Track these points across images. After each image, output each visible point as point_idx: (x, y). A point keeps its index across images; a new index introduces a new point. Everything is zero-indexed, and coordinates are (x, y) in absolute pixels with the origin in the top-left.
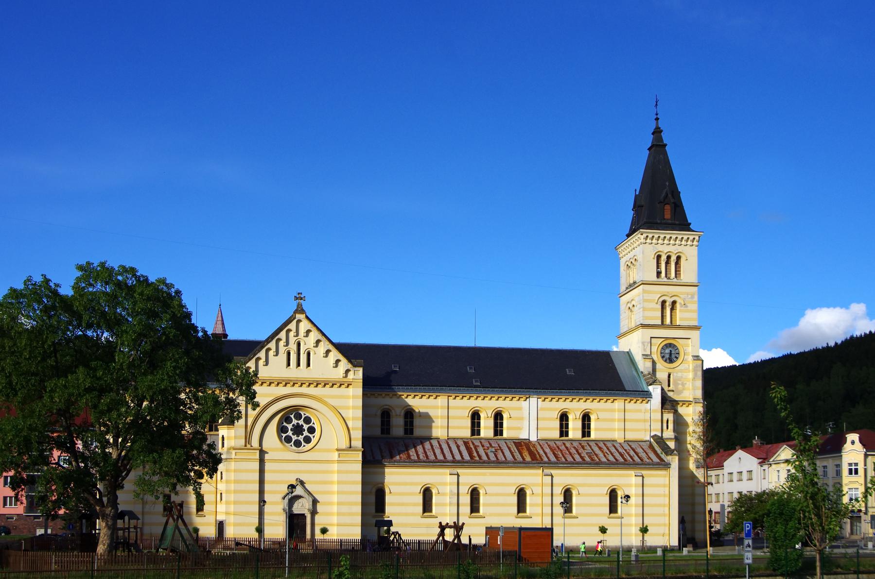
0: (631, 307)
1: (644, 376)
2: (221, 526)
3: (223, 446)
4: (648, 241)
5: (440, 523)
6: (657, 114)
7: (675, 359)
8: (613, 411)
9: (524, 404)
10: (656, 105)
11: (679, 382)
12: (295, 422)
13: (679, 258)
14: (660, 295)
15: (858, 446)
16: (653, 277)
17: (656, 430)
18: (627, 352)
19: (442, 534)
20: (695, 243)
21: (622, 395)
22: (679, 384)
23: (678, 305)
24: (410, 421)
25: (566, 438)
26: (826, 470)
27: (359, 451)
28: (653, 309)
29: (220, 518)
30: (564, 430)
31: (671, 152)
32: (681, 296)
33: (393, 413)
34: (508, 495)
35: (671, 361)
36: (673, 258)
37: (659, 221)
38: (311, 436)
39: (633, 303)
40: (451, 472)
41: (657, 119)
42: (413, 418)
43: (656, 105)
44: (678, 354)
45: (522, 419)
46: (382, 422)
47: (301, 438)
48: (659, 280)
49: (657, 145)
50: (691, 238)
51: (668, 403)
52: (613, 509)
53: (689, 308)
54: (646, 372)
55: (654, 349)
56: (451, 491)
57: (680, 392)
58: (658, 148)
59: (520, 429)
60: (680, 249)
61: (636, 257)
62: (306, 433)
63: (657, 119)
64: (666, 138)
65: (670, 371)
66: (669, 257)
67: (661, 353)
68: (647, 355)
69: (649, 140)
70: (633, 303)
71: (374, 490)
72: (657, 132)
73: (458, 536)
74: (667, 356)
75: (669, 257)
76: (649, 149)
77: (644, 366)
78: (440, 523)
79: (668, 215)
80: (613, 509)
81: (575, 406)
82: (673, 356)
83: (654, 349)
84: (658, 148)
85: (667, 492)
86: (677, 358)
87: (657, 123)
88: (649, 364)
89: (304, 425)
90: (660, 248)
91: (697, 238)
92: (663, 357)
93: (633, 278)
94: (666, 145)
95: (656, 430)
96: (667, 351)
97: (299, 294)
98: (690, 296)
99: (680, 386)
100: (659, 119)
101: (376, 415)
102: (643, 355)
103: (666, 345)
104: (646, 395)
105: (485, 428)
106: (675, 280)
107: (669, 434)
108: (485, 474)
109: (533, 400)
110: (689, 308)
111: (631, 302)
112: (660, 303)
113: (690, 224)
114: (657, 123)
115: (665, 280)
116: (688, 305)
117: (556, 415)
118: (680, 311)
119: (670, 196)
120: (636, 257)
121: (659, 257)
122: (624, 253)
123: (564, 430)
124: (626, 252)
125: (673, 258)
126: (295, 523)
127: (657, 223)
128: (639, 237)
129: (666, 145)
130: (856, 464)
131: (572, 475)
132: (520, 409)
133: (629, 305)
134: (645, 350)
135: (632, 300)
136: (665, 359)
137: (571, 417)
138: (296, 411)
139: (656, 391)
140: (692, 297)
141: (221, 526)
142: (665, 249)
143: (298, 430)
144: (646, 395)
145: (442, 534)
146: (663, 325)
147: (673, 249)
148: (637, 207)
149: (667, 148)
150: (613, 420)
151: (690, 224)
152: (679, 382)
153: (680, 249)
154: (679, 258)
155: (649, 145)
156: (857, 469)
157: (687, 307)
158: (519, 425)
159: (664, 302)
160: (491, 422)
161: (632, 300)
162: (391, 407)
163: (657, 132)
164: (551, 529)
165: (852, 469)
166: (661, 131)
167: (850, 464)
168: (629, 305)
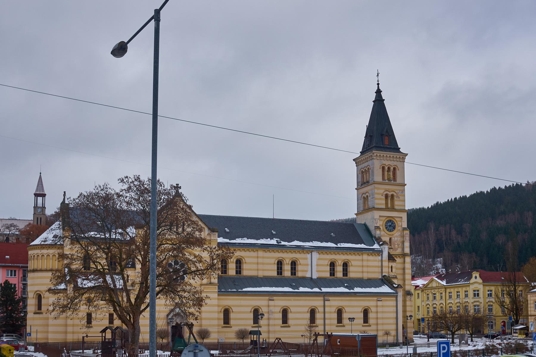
0: (365, 196)
6: (378, 81)
10: (378, 75)
11: (396, 243)
13: (394, 169)
15: (479, 280)
17: (385, 273)
18: (364, 224)
22: (395, 245)
24: (333, 268)
26: (451, 294)
27: (216, 285)
28: (381, 199)
30: (332, 273)
31: (387, 104)
34: (304, 313)
36: (392, 168)
39: (367, 194)
40: (270, 299)
41: (378, 84)
42: (296, 266)
43: (378, 75)
44: (395, 226)
45: (307, 265)
53: (401, 199)
57: (396, 249)
59: (306, 271)
61: (369, 167)
63: (378, 84)
64: (384, 95)
65: (391, 236)
66: (389, 168)
67: (385, 226)
69: (373, 97)
70: (367, 194)
72: (379, 92)
75: (389, 168)
90: (384, 162)
92: (386, 228)
93: (366, 179)
94: (384, 100)
95: (385, 273)
97: (177, 184)
98: (401, 192)
99: (396, 246)
100: (379, 84)
101: (275, 263)
102: (375, 226)
103: (388, 221)
106: (392, 182)
108: (300, 300)
110: (401, 199)
111: (365, 194)
112: (384, 195)
113: (400, 148)
116: (400, 197)
120: (369, 167)
121: (383, 168)
123: (332, 273)
125: (392, 168)
129: (384, 100)
130: (478, 291)
131: (342, 300)
132: (306, 259)
133: (364, 195)
135: (366, 193)
136: (387, 229)
139: (386, 250)
142: (387, 163)
146: (387, 209)
149: (385, 102)
151: (400, 148)
153: (395, 163)
154: (394, 169)
156: (479, 293)
157: (399, 198)
158: (306, 269)
161: (366, 193)
162: (335, 260)
163: (379, 92)
165: (476, 293)
167: (474, 291)
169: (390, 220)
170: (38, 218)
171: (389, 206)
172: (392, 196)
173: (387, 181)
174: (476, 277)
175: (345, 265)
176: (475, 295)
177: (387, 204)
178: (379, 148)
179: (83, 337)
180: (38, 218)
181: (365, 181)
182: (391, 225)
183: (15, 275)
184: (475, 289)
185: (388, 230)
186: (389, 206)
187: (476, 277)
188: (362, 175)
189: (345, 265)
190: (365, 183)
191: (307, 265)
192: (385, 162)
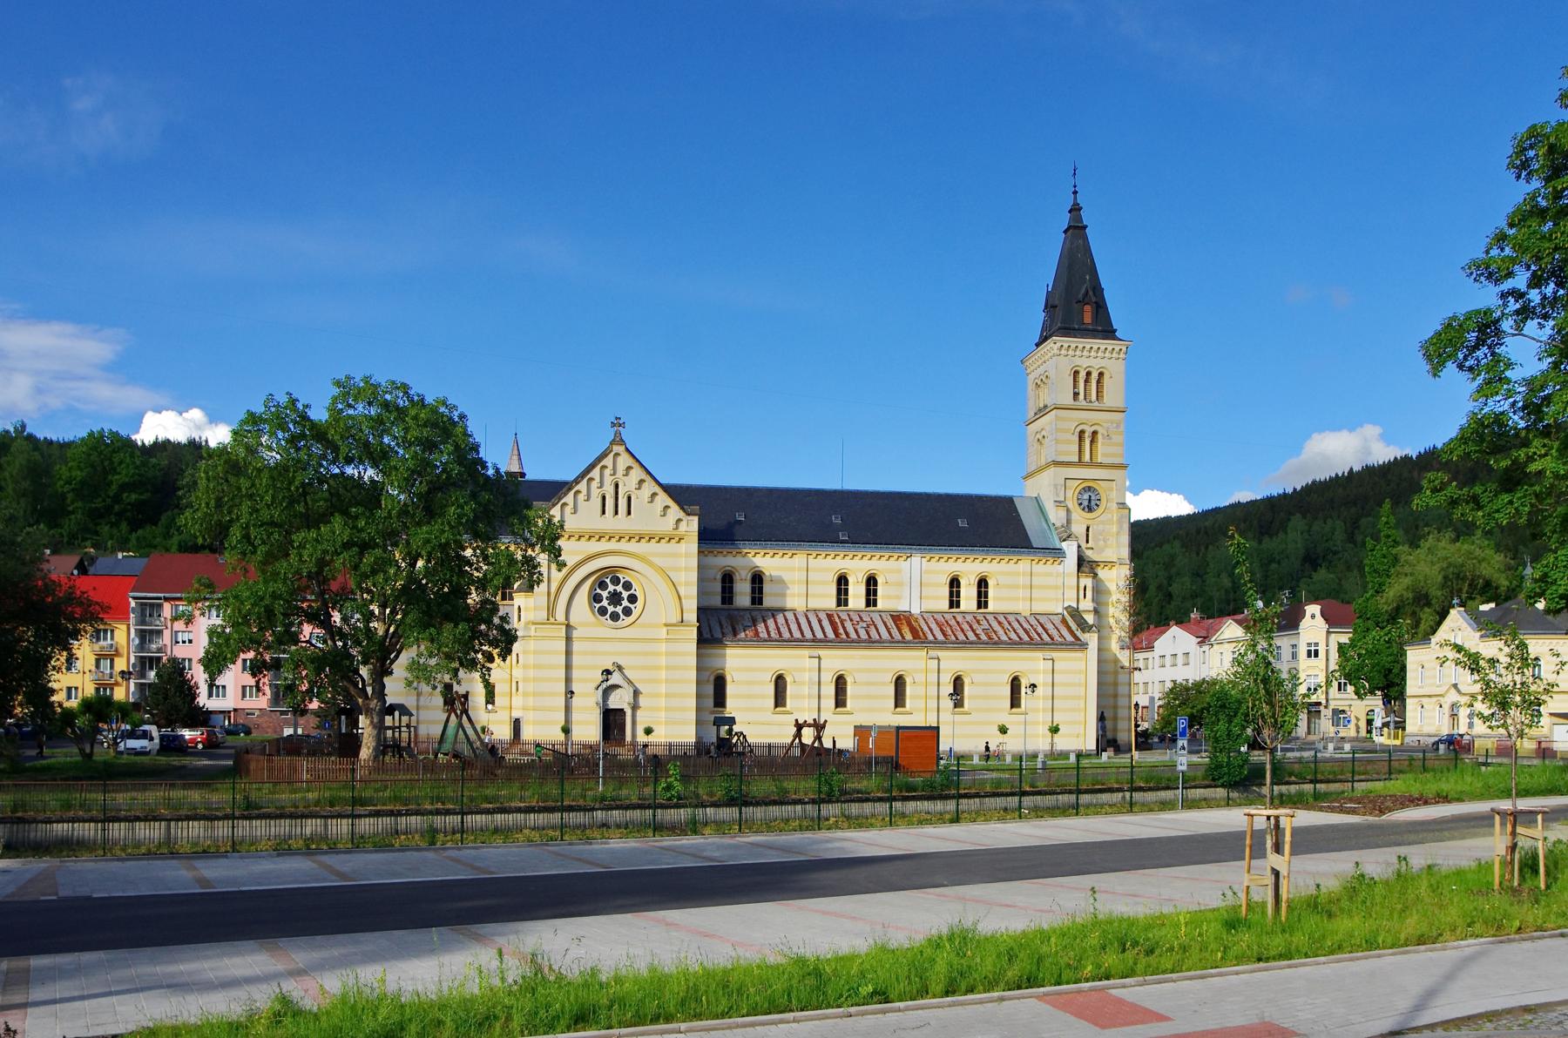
0: (1041, 438)
1: (1056, 529)
2: (517, 724)
3: (519, 620)
4: (1063, 352)
5: (797, 720)
6: (1075, 186)
7: (1095, 507)
8: (1018, 574)
9: (903, 565)
12: (611, 588)
13: (1101, 374)
16: (1069, 400)
19: (798, 734)
20: (1122, 355)
21: (1029, 553)
22: (1099, 540)
23: (1100, 436)
25: (957, 610)
28: (1069, 442)
29: (516, 714)
30: (954, 602)
32: (1104, 425)
33: (737, 577)
35: (1090, 509)
36: (1095, 375)
37: (1077, 327)
38: (632, 606)
39: (1044, 433)
41: (1075, 193)
46: (724, 589)
47: (619, 609)
48: (1076, 403)
49: (1076, 227)
50: (1117, 349)
51: (1084, 564)
52: (1015, 702)
54: (1058, 524)
55: (1070, 494)
56: (810, 679)
57: (1102, 551)
58: (1076, 230)
59: (899, 597)
60: (1103, 363)
62: (625, 603)
63: (1075, 193)
65: (1089, 522)
66: (1089, 374)
68: (1060, 502)
70: (1044, 433)
71: (712, 678)
72: (1075, 209)
73: (819, 738)
74: (1086, 503)
75: (1089, 374)
76: (1065, 232)
77: (1056, 516)
78: (797, 720)
79: (1088, 318)
80: (1015, 702)
81: (969, 567)
82: (1093, 503)
83: (1070, 494)
84: (1076, 230)
85: (1083, 681)
86: (1098, 506)
87: (1075, 198)
88: (1063, 513)
89: (623, 592)
90: (1078, 361)
91: (1124, 349)
96: (1086, 496)
104: (1058, 553)
105: (855, 596)
107: (1087, 605)
113: (1115, 331)
114: (1075, 198)
115: (1084, 403)
117: (945, 580)
118: (1103, 444)
119: (1091, 293)
121: (1076, 373)
122: (1032, 368)
123: (954, 602)
124: (1035, 366)
125: (1095, 375)
126: (612, 721)
127: (1074, 329)
129: (1085, 227)
132: (899, 571)
133: (1038, 436)
134: (1057, 495)
138: (612, 574)
139: (1070, 549)
140: (1118, 426)
141: (517, 724)
142: (1083, 363)
143: (615, 598)
144: (1058, 553)
145: (798, 734)
146: (1080, 463)
147: (1095, 364)
148: (1050, 307)
149: (1087, 230)
150: (1017, 587)
151: (1115, 331)
154: (1101, 374)
157: (1110, 439)
159: (1082, 432)
160: (862, 589)
163: (1075, 209)
164: (938, 728)
169: (1089, 488)
171: (1087, 458)
172: (1095, 433)
173: (1081, 401)
177: (1080, 451)
178: (1067, 331)
185: (1083, 509)
186: (1087, 458)
191: (900, 584)
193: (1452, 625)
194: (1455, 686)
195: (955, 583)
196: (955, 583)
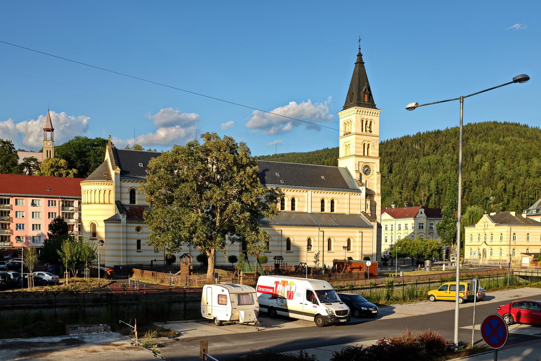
0: (347, 145)
1: (356, 181)
4: (358, 112)
7: (369, 173)
8: (344, 199)
9: (305, 194)
14: (363, 141)
15: (424, 215)
16: (360, 132)
20: (378, 115)
21: (349, 191)
23: (370, 146)
34: (304, 241)
37: (362, 103)
39: (349, 143)
48: (363, 133)
50: (377, 113)
51: (369, 194)
54: (357, 180)
56: (278, 239)
59: (303, 207)
65: (367, 179)
68: (357, 171)
75: (367, 121)
76: (356, 64)
77: (355, 176)
79: (366, 100)
81: (328, 196)
85: (372, 240)
86: (370, 173)
88: (358, 175)
90: (363, 116)
91: (379, 113)
94: (364, 63)
95: (362, 209)
102: (356, 171)
103: (365, 166)
104: (359, 191)
107: (368, 211)
109: (310, 192)
112: (363, 145)
113: (375, 105)
115: (365, 133)
117: (319, 200)
118: (372, 149)
119: (367, 90)
122: (342, 116)
123: (323, 210)
124: (344, 116)
128: (353, 110)
129: (364, 63)
130: (422, 224)
131: (332, 232)
132: (303, 196)
134: (356, 168)
137: (326, 201)
139: (363, 189)
142: (365, 117)
144: (359, 191)
147: (369, 118)
149: (364, 64)
150: (344, 204)
152: (371, 185)
153: (372, 117)
154: (371, 122)
155: (355, 62)
157: (374, 147)
159: (364, 144)
160: (290, 203)
161: (348, 141)
166: (362, 55)
167: (420, 224)
168: (346, 144)
170: (47, 151)
171: (366, 154)
174: (421, 213)
175: (332, 202)
176: (420, 226)
178: (360, 103)
179: (152, 261)
180: (47, 151)
181: (347, 131)
182: (367, 170)
183: (55, 205)
184: (420, 223)
186: (366, 154)
187: (421, 213)
188: (345, 126)
189: (332, 202)
190: (347, 134)
191: (304, 202)
192: (363, 116)
193: (484, 220)
194: (485, 242)
195: (323, 202)
196: (323, 202)
